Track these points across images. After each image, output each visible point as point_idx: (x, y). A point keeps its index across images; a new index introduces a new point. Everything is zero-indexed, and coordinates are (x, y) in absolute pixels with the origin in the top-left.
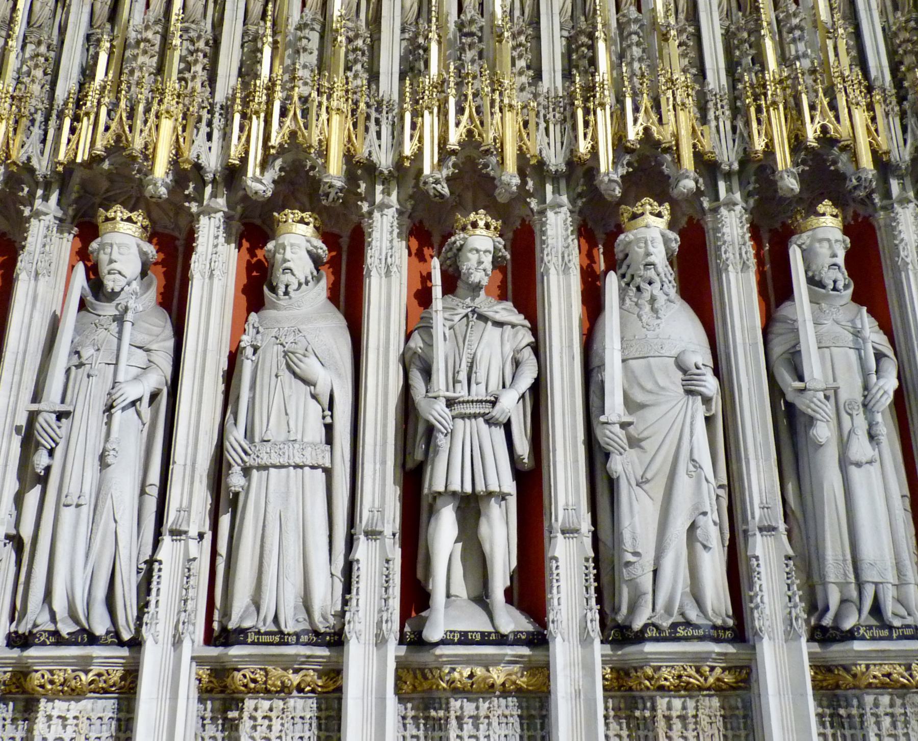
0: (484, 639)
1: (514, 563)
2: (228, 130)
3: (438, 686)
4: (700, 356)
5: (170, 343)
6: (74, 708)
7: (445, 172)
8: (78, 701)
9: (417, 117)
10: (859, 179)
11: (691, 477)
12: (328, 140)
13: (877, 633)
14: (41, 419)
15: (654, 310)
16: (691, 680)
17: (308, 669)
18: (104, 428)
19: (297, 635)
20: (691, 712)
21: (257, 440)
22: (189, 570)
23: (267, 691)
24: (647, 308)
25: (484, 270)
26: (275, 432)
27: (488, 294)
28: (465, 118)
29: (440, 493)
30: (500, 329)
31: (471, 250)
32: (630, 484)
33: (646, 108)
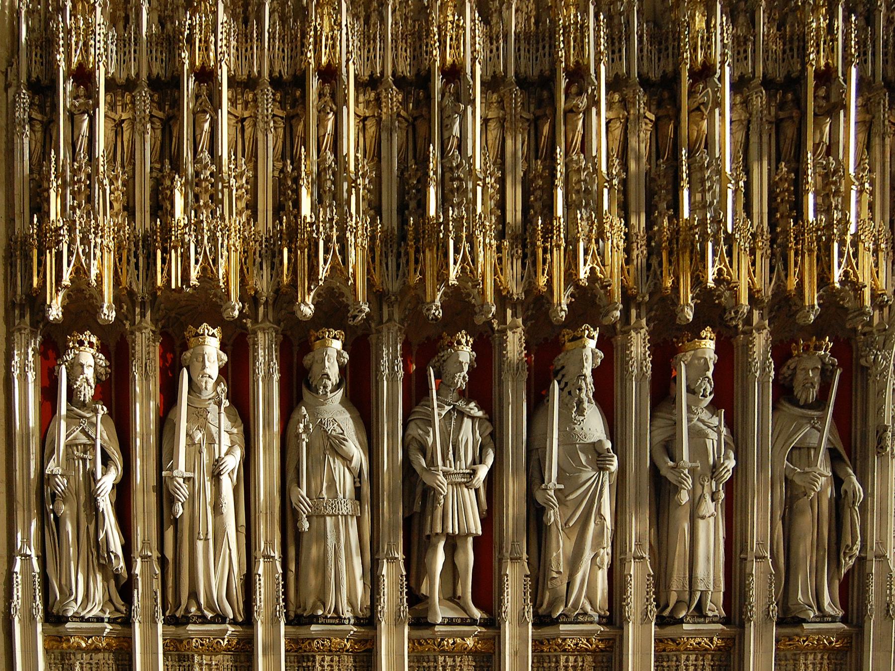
8: (216, 655)
13: (696, 620)
23: (330, 651)
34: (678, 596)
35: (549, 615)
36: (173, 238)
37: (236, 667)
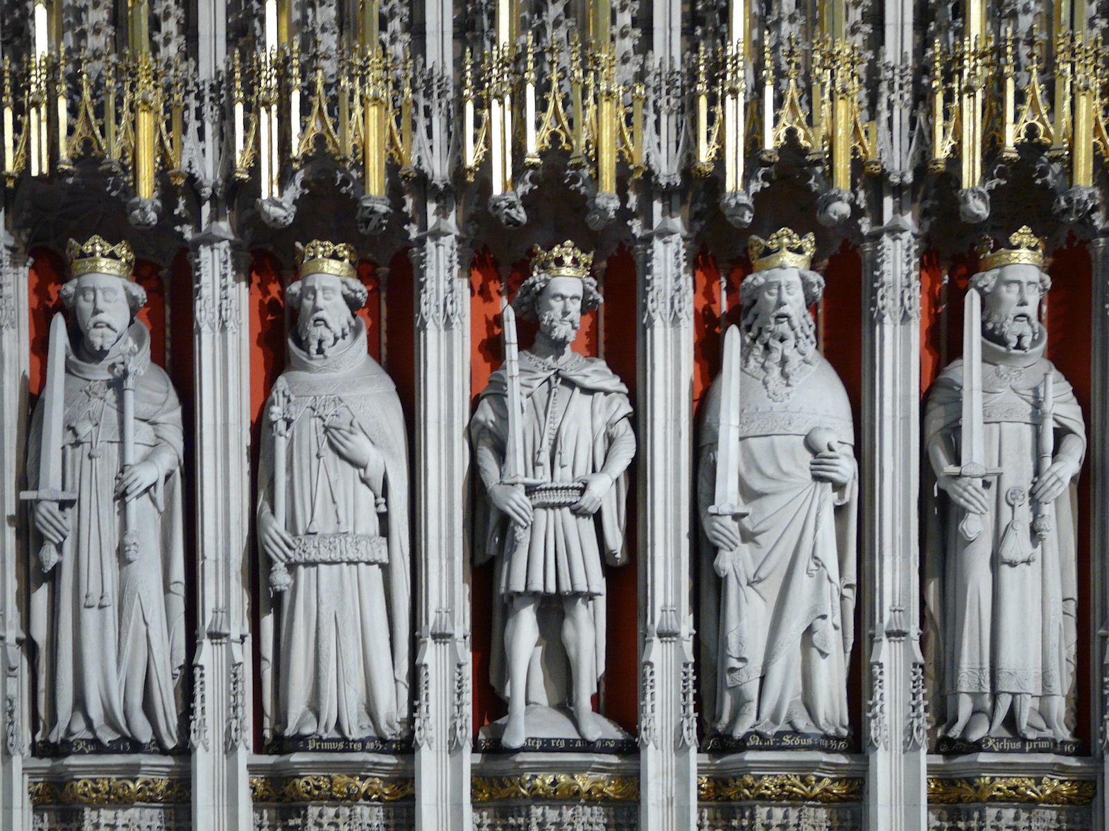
0: (570, 746)
1: (602, 669)
3: (518, 792)
7: (522, 189)
9: (482, 108)
11: (811, 576)
13: (1007, 745)
15: (784, 375)
16: (795, 789)
17: (374, 777)
19: (363, 742)
21: (301, 531)
24: (776, 371)
25: (572, 322)
27: (574, 350)
29: (519, 594)
30: (591, 397)
31: (555, 296)
32: (739, 583)
33: (792, 100)
34: (974, 702)
35: (730, 737)
36: (33, 89)
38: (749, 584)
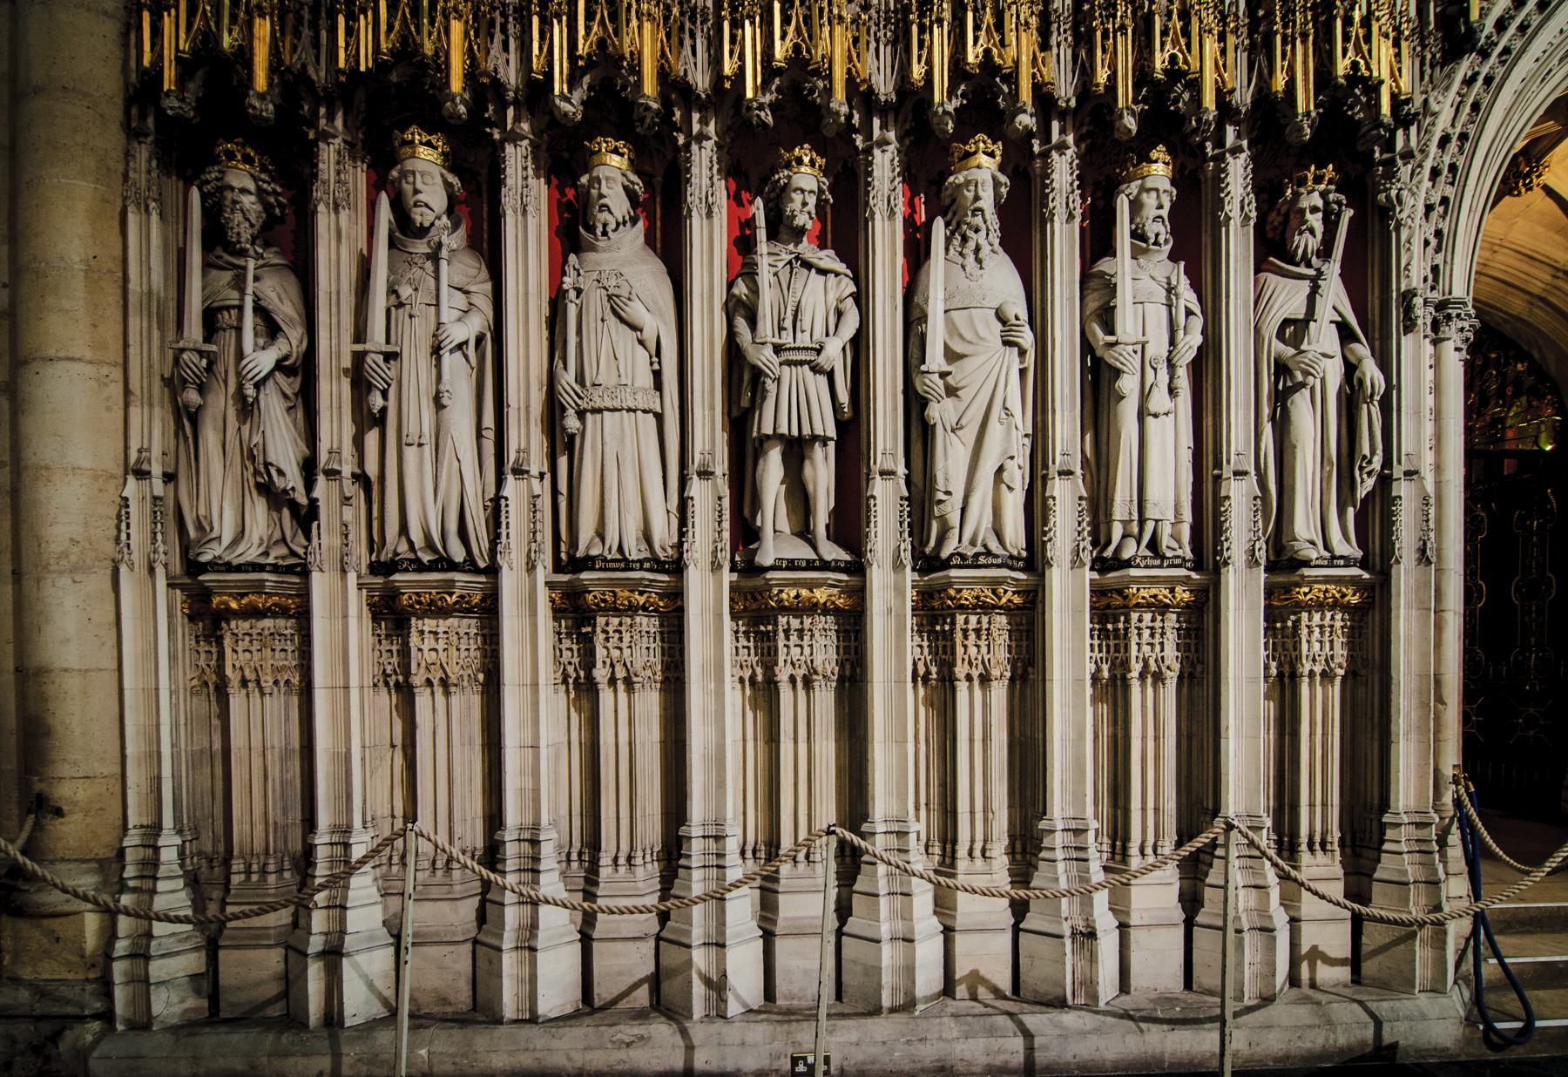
0: (809, 566)
2: (527, 38)
3: (767, 604)
4: (1017, 308)
5: (488, 287)
6: (443, 625)
9: (737, 28)
10: (1199, 120)
11: (1002, 424)
12: (640, 53)
13: (1150, 562)
14: (369, 360)
15: (979, 261)
18: (434, 371)
19: (641, 562)
20: (985, 626)
21: (588, 384)
22: (535, 506)
23: (616, 609)
24: (971, 258)
26: (606, 377)
28: (791, 29)
29: (768, 436)
30: (823, 278)
31: (796, 190)
33: (988, 25)
34: (1124, 528)
35: (938, 557)
37: (483, 635)
38: (953, 431)
